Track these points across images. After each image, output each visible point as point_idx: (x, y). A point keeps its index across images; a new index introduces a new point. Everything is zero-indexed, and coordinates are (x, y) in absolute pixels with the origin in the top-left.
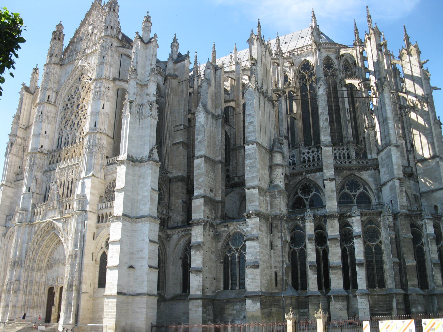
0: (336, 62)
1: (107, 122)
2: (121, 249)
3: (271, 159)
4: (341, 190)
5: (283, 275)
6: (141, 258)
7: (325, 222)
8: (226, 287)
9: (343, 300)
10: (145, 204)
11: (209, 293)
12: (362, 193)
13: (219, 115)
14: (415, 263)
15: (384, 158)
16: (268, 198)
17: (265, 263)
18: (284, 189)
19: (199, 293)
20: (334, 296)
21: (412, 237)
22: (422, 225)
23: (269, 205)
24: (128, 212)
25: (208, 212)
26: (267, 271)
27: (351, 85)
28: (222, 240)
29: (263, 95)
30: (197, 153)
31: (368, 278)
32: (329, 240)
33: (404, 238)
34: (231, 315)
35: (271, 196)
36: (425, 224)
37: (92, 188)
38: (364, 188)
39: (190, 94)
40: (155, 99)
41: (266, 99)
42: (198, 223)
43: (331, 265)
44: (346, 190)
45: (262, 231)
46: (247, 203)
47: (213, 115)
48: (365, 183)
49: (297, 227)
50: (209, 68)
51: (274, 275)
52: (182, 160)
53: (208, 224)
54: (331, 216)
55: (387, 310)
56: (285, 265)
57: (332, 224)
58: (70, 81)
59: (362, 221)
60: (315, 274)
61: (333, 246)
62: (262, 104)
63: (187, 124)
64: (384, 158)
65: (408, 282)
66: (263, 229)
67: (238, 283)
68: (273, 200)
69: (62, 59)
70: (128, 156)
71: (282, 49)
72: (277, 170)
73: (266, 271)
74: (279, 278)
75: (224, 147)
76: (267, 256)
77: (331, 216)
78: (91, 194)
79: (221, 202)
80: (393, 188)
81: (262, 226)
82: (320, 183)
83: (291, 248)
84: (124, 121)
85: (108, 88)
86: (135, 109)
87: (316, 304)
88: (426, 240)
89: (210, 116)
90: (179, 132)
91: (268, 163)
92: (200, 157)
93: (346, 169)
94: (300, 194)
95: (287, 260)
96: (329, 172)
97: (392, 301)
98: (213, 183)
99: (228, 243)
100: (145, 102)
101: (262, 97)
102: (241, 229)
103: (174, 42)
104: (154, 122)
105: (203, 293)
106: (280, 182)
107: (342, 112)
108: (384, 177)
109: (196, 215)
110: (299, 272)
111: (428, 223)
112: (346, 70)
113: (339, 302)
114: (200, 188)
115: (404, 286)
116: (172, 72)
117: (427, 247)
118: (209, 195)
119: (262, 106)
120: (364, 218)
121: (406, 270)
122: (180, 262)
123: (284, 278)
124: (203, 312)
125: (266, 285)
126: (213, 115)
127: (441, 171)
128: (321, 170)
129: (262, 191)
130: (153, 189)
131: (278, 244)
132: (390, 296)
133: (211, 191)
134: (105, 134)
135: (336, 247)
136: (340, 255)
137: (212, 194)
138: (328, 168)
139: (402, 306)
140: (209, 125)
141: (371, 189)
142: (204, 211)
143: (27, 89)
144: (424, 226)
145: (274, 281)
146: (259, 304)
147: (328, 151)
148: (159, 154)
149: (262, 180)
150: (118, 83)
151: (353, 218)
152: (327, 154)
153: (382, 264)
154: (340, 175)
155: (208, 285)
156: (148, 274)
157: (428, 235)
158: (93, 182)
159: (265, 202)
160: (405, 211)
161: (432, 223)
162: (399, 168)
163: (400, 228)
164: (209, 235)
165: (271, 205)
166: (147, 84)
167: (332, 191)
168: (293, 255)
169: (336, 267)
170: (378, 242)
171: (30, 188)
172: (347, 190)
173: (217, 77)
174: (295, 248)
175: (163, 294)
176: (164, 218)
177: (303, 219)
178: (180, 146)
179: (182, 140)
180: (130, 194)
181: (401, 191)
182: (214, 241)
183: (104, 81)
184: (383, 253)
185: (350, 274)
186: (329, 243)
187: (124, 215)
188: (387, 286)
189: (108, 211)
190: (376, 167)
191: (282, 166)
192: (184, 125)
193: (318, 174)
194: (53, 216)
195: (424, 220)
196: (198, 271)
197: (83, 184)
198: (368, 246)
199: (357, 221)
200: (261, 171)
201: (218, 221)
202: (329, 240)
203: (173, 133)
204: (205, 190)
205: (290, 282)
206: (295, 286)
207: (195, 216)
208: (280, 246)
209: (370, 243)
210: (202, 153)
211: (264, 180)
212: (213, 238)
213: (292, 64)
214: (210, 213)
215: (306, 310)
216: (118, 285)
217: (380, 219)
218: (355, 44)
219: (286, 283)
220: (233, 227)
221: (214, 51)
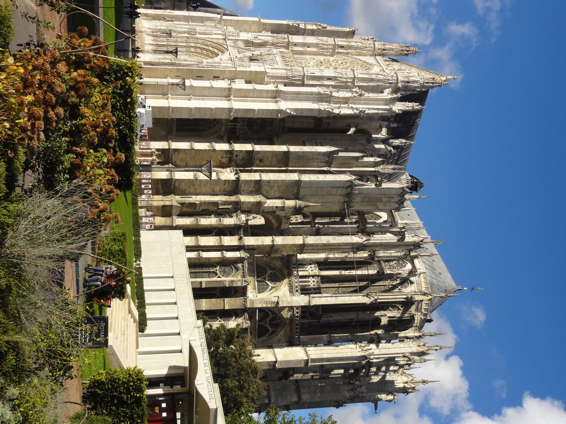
4: (269, 267)
17: (198, 187)
25: (241, 156)
32: (221, 239)
38: (273, 287)
41: (347, 200)
44: (269, 272)
45: (225, 184)
57: (233, 240)
60: (191, 222)
62: (339, 192)
66: (227, 185)
73: (192, 187)
78: (251, 72)
81: (229, 184)
87: (166, 222)
93: (288, 271)
101: (345, 192)
105: (174, 149)
114: (260, 148)
119: (336, 191)
125: (181, 188)
133: (261, 161)
135: (214, 242)
137: (258, 162)
138: (283, 239)
140: (318, 157)
141: (271, 293)
142: (241, 151)
147: (299, 240)
149: (268, 187)
152: (296, 240)
154: (283, 265)
162: (289, 303)
170: (219, 275)
171: (257, 37)
172: (269, 272)
175: (173, 134)
182: (218, 163)
194: (233, 52)
200: (276, 185)
211: (268, 189)
214: (241, 158)
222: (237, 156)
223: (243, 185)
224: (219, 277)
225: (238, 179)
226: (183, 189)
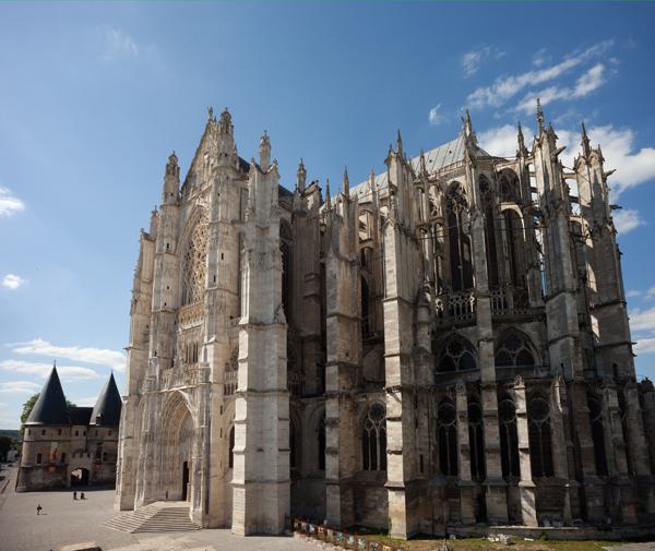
0: (492, 180)
1: (228, 277)
2: (247, 429)
3: (415, 315)
7: (480, 393)
8: (366, 467)
9: (502, 492)
10: (272, 375)
11: (347, 475)
12: (524, 352)
13: (354, 261)
14: (591, 445)
15: (554, 307)
16: (412, 366)
18: (430, 351)
20: (491, 487)
22: (602, 396)
24: (253, 387)
25: (343, 382)
27: (509, 210)
28: (360, 413)
30: (329, 311)
32: (486, 416)
33: (580, 413)
34: (372, 500)
35: (415, 362)
36: (607, 393)
37: (215, 355)
38: (526, 345)
39: (322, 233)
40: (277, 245)
43: (487, 446)
44: (505, 349)
46: (388, 375)
47: (347, 261)
48: (528, 338)
49: (446, 399)
51: (419, 459)
52: (314, 316)
54: (488, 387)
55: (557, 506)
63: (318, 272)
64: (554, 307)
65: (584, 469)
67: (379, 464)
69: (178, 199)
70: (250, 318)
71: (427, 168)
74: (425, 463)
78: (215, 362)
80: (564, 348)
82: (473, 340)
83: (438, 425)
84: (244, 276)
85: (227, 233)
86: (256, 260)
88: (606, 414)
89: (343, 264)
90: (310, 283)
92: (332, 315)
94: (448, 353)
96: (486, 331)
99: (367, 417)
100: (267, 250)
103: (300, 170)
104: (279, 275)
106: (426, 344)
107: (498, 246)
108: (553, 333)
112: (504, 192)
114: (333, 354)
115: (579, 476)
116: (299, 207)
117: (608, 424)
120: (530, 390)
122: (317, 435)
124: (341, 500)
126: (347, 261)
128: (474, 323)
130: (280, 358)
131: (425, 422)
133: (347, 355)
134: (227, 290)
136: (498, 435)
139: (577, 503)
141: (533, 345)
143: (146, 236)
144: (605, 397)
145: (419, 466)
146: (403, 498)
148: (286, 313)
150: (236, 226)
155: (345, 467)
156: (278, 458)
157: (610, 409)
158: (215, 349)
160: (580, 378)
165: (416, 374)
166: (268, 228)
168: (441, 433)
169: (492, 451)
172: (505, 349)
180: (255, 363)
181: (577, 353)
183: (221, 225)
185: (510, 458)
187: (249, 390)
190: (542, 317)
193: (470, 328)
196: (334, 452)
197: (206, 350)
198: (534, 424)
201: (354, 391)
202: (486, 416)
204: (340, 356)
205: (437, 466)
206: (444, 470)
207: (329, 387)
208: (426, 424)
209: (535, 421)
210: (334, 311)
212: (351, 411)
213: (439, 188)
215: (457, 500)
216: (246, 472)
218: (518, 156)
219: (434, 467)
220: (372, 399)
221: (346, 178)
223: (406, 382)
224: (549, 420)
225: (400, 389)
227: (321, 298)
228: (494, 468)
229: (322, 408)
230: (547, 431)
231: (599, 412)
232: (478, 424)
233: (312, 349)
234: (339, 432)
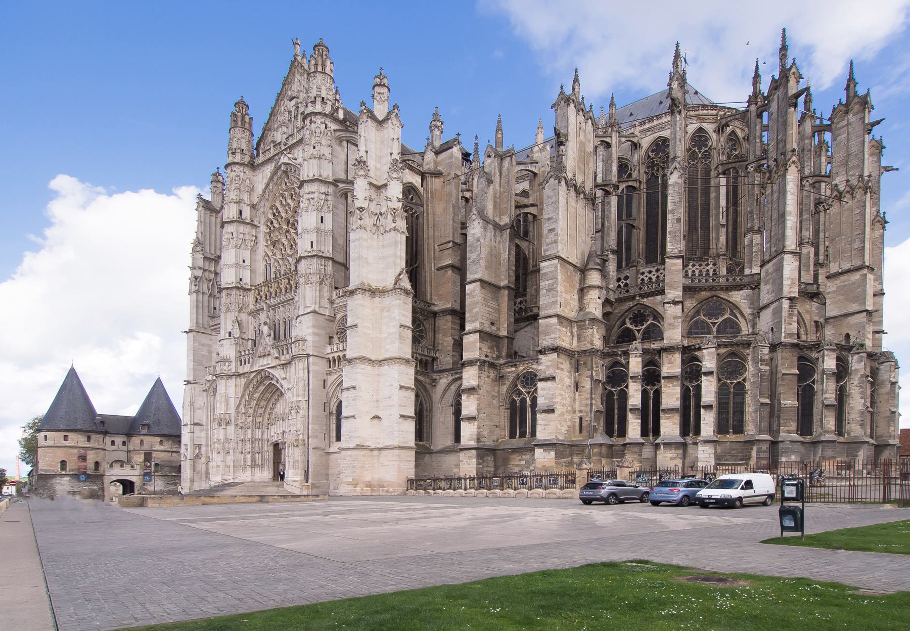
5: (591, 421)
6: (392, 406)
16: (575, 330)
19: (473, 443)
20: (664, 444)
21: (797, 372)
23: (575, 338)
25: (486, 349)
26: (568, 417)
29: (576, 191)
31: (719, 422)
42: (471, 363)
50: (489, 156)
51: (578, 421)
53: (486, 364)
56: (594, 408)
58: (271, 188)
59: (718, 354)
61: (668, 385)
68: (582, 331)
72: (591, 293)
74: (585, 424)
75: (514, 268)
76: (568, 400)
77: (669, 350)
79: (507, 337)
87: (636, 452)
88: (819, 377)
90: (447, 252)
91: (578, 285)
95: (599, 403)
97: (752, 449)
98: (495, 315)
102: (534, 369)
106: (595, 308)
109: (469, 353)
110: (616, 417)
111: (827, 356)
113: (671, 450)
118: (488, 330)
121: (780, 413)
123: (592, 424)
127: (867, 286)
128: (662, 292)
129: (564, 320)
132: (751, 443)
133: (492, 324)
137: (494, 328)
139: (766, 455)
144: (820, 359)
151: (704, 351)
153: (743, 407)
157: (823, 371)
159: (569, 334)
161: (834, 355)
163: (780, 362)
164: (488, 377)
167: (675, 318)
168: (608, 398)
173: (504, 169)
174: (612, 389)
176: (426, 360)
177: (626, 354)
178: (448, 269)
179: (450, 262)
184: (746, 393)
186: (663, 381)
188: (746, 433)
189: (341, 354)
191: (600, 288)
192: (453, 242)
195: (822, 352)
199: (709, 354)
201: (502, 361)
203: (437, 253)
207: (467, 356)
214: (489, 351)
217: (748, 351)
222: (486, 356)
226: (567, 429)
227: (460, 269)
228: (670, 427)
229: (459, 382)
230: (740, 389)
231: (812, 376)
232: (655, 388)
233: (446, 324)
234: (479, 399)
